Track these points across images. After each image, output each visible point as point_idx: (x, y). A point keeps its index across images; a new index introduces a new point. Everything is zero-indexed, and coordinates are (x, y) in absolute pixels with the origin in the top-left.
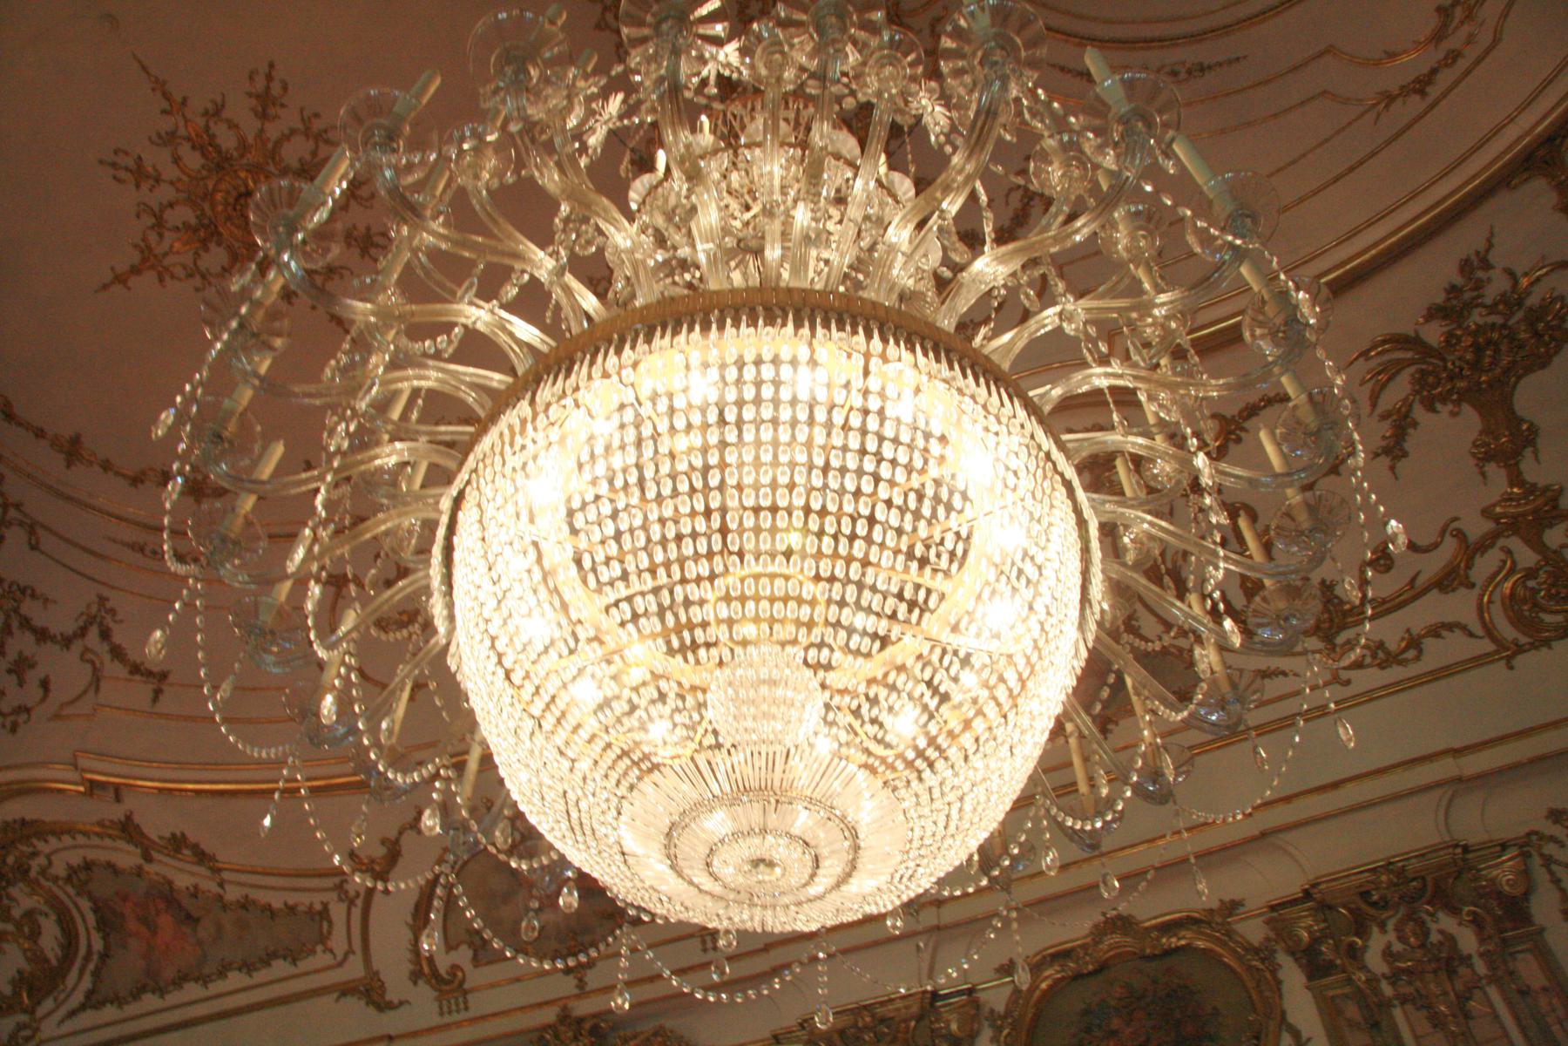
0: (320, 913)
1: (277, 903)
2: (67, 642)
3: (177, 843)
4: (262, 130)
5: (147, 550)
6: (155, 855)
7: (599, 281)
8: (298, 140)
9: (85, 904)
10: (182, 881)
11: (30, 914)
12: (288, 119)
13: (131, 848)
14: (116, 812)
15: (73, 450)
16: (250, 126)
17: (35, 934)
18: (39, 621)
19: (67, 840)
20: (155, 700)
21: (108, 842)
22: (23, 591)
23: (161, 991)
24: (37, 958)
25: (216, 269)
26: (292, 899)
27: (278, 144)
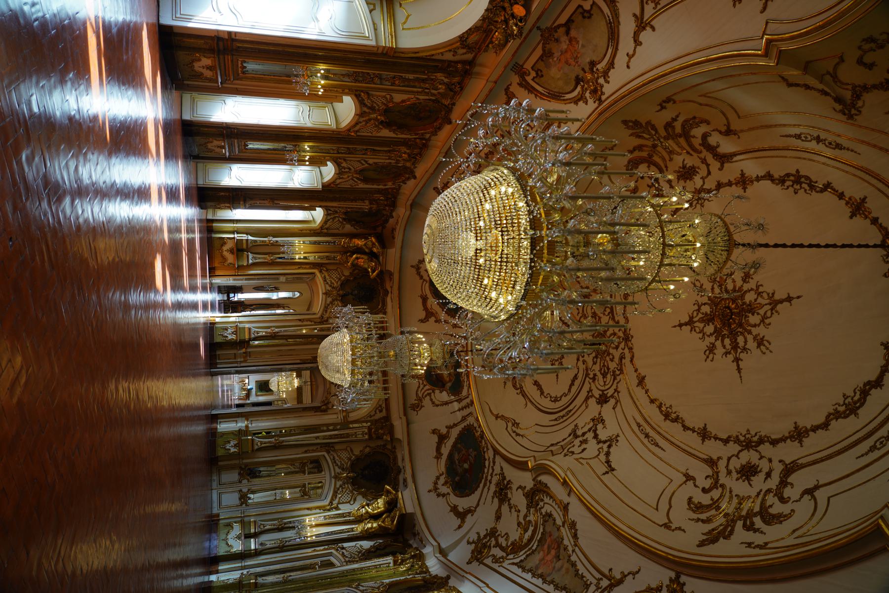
0: (587, 585)
1: (580, 572)
2: (599, 442)
3: (573, 525)
4: (742, 286)
5: (641, 428)
6: (566, 526)
7: (848, 397)
8: (752, 293)
9: (541, 530)
10: (566, 542)
11: (530, 522)
12: (752, 284)
13: (562, 517)
14: (566, 499)
15: (641, 381)
16: (739, 283)
17: (526, 530)
18: (598, 432)
19: (550, 502)
20: (604, 474)
21: (558, 510)
22: (602, 420)
23: (534, 576)
24: (521, 539)
25: (709, 334)
26: (586, 574)
27: (746, 292)
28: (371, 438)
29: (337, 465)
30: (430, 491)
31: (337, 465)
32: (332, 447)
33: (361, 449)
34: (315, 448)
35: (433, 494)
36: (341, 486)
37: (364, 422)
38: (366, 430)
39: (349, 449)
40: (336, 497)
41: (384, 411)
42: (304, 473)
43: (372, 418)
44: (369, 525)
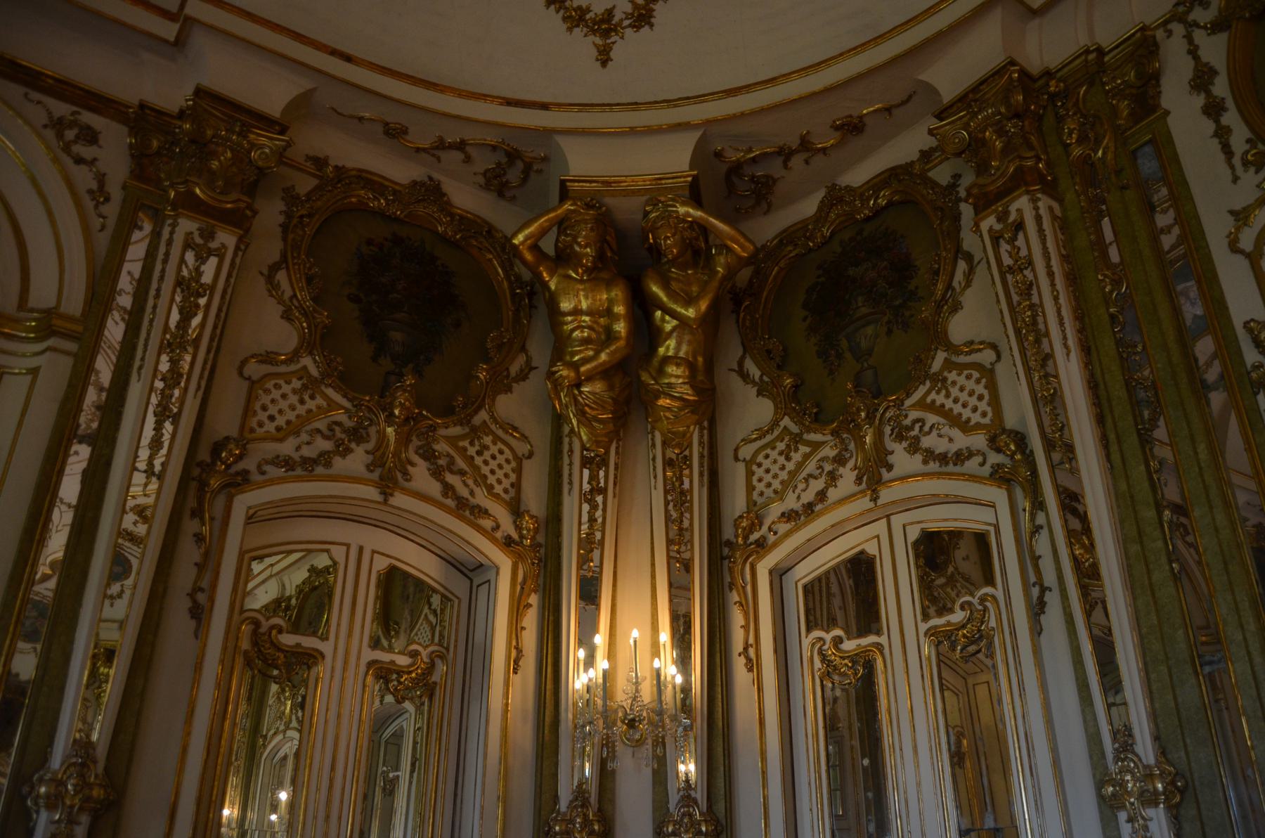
28: (240, 220)
29: (324, 459)
30: (604, 57)
31: (324, 459)
32: (217, 448)
33: (273, 310)
34: (189, 553)
35: (628, 45)
36: (437, 473)
37: (120, 244)
38: (187, 225)
39: (254, 369)
40: (485, 513)
41: (88, 118)
42: (310, 658)
43: (116, 194)
44: (675, 373)
